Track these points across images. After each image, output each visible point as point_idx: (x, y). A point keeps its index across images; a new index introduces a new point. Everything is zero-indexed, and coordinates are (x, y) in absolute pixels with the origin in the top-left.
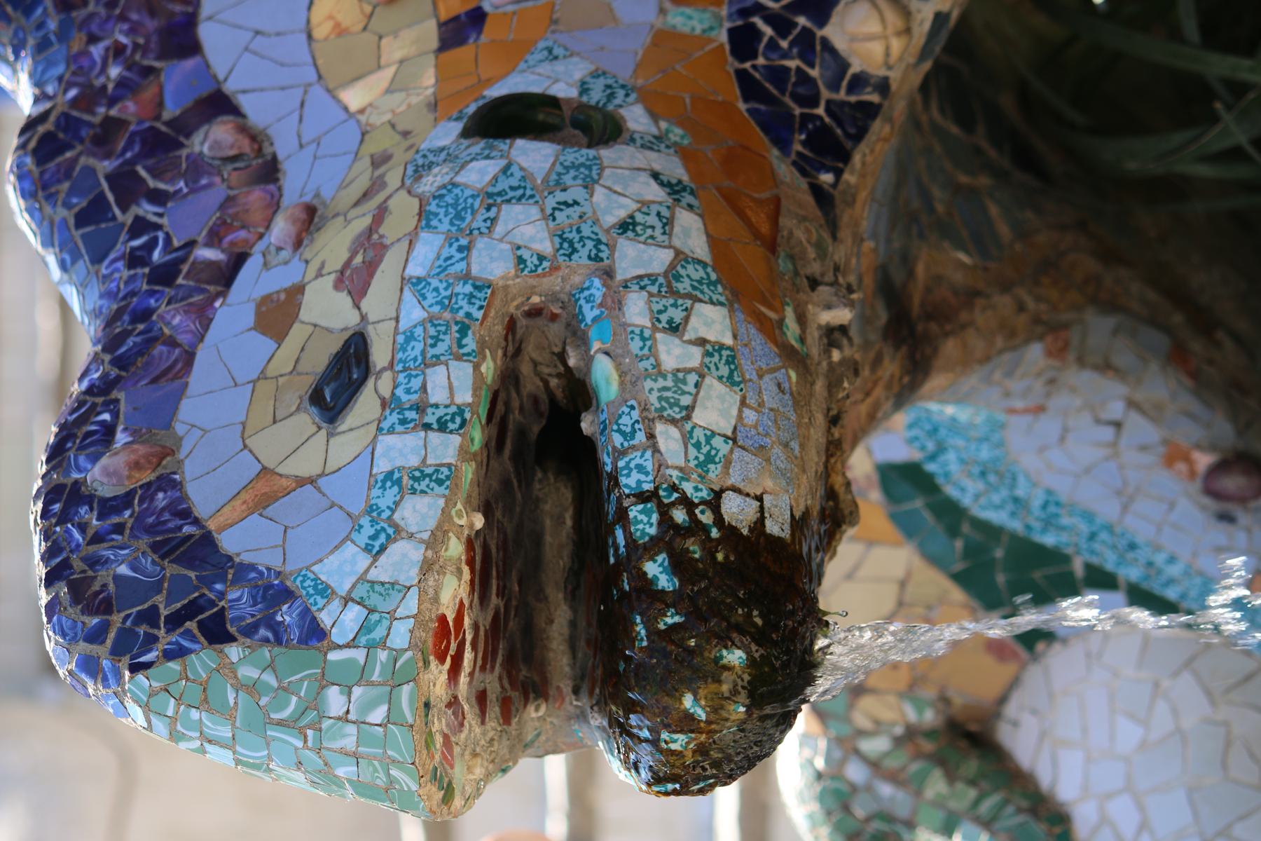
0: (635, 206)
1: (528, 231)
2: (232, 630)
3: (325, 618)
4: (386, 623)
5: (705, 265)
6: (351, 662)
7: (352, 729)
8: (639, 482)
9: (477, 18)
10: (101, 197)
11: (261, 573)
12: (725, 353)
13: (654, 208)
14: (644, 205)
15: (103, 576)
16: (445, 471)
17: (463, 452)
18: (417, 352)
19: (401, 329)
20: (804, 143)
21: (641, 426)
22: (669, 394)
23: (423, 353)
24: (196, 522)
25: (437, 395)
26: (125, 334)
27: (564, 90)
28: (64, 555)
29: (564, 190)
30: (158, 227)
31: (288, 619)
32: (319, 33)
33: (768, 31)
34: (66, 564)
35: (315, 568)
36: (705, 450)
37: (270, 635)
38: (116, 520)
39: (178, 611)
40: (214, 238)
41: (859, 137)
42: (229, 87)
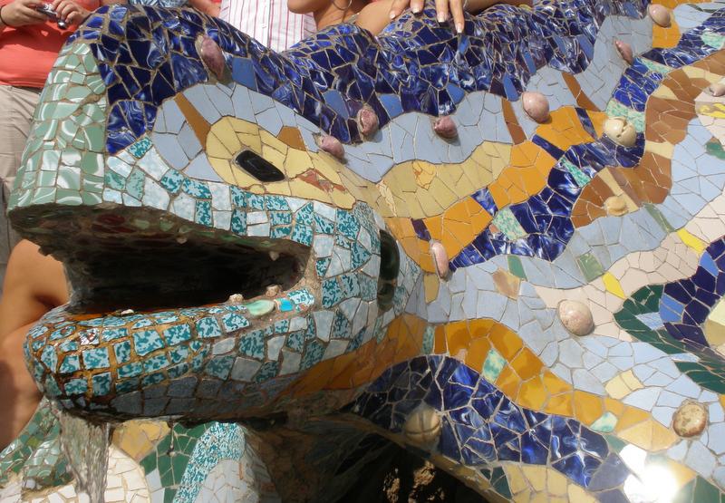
0: (350, 319)
2: (117, 103)
3: (123, 154)
4: (119, 188)
5: (320, 358)
6: (95, 167)
7: (54, 167)
8: (203, 329)
10: (342, 62)
11: (150, 120)
12: (274, 372)
13: (349, 330)
14: (351, 323)
15: (149, 37)
16: (209, 222)
17: (222, 232)
18: (275, 207)
19: (287, 199)
20: (373, 397)
21: (235, 329)
22: (252, 344)
23: (274, 210)
24: (182, 88)
25: (252, 218)
26: (280, 65)
27: (400, 279)
28: (162, 18)
29: (358, 283)
30: (330, 86)
31: (123, 133)
33: (423, 376)
34: (157, 19)
35: (153, 149)
36: (221, 365)
37: (113, 123)
38: (182, 46)
39: (128, 73)
40: (325, 111)
41: (374, 421)
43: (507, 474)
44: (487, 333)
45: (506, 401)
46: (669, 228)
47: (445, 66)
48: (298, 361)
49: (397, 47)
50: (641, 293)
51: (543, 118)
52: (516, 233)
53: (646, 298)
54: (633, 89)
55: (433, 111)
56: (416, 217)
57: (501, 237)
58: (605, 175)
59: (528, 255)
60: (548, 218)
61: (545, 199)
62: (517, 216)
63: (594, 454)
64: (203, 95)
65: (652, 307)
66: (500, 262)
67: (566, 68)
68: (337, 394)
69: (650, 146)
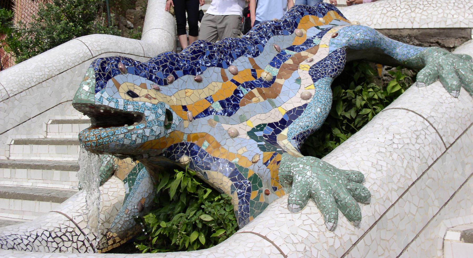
3: (98, 93)
24: (113, 76)
25: (129, 107)
26: (142, 67)
32: (186, 90)
34: (109, 60)
40: (156, 78)
42: (179, 79)
44: (205, 136)
45: (208, 155)
46: (274, 106)
47: (200, 61)
48: (141, 140)
50: (259, 126)
51: (235, 74)
53: (261, 127)
54: (278, 60)
55: (194, 74)
56: (183, 105)
58: (255, 91)
59: (221, 115)
60: (231, 104)
62: (220, 104)
65: (262, 130)
66: (211, 117)
69: (277, 81)
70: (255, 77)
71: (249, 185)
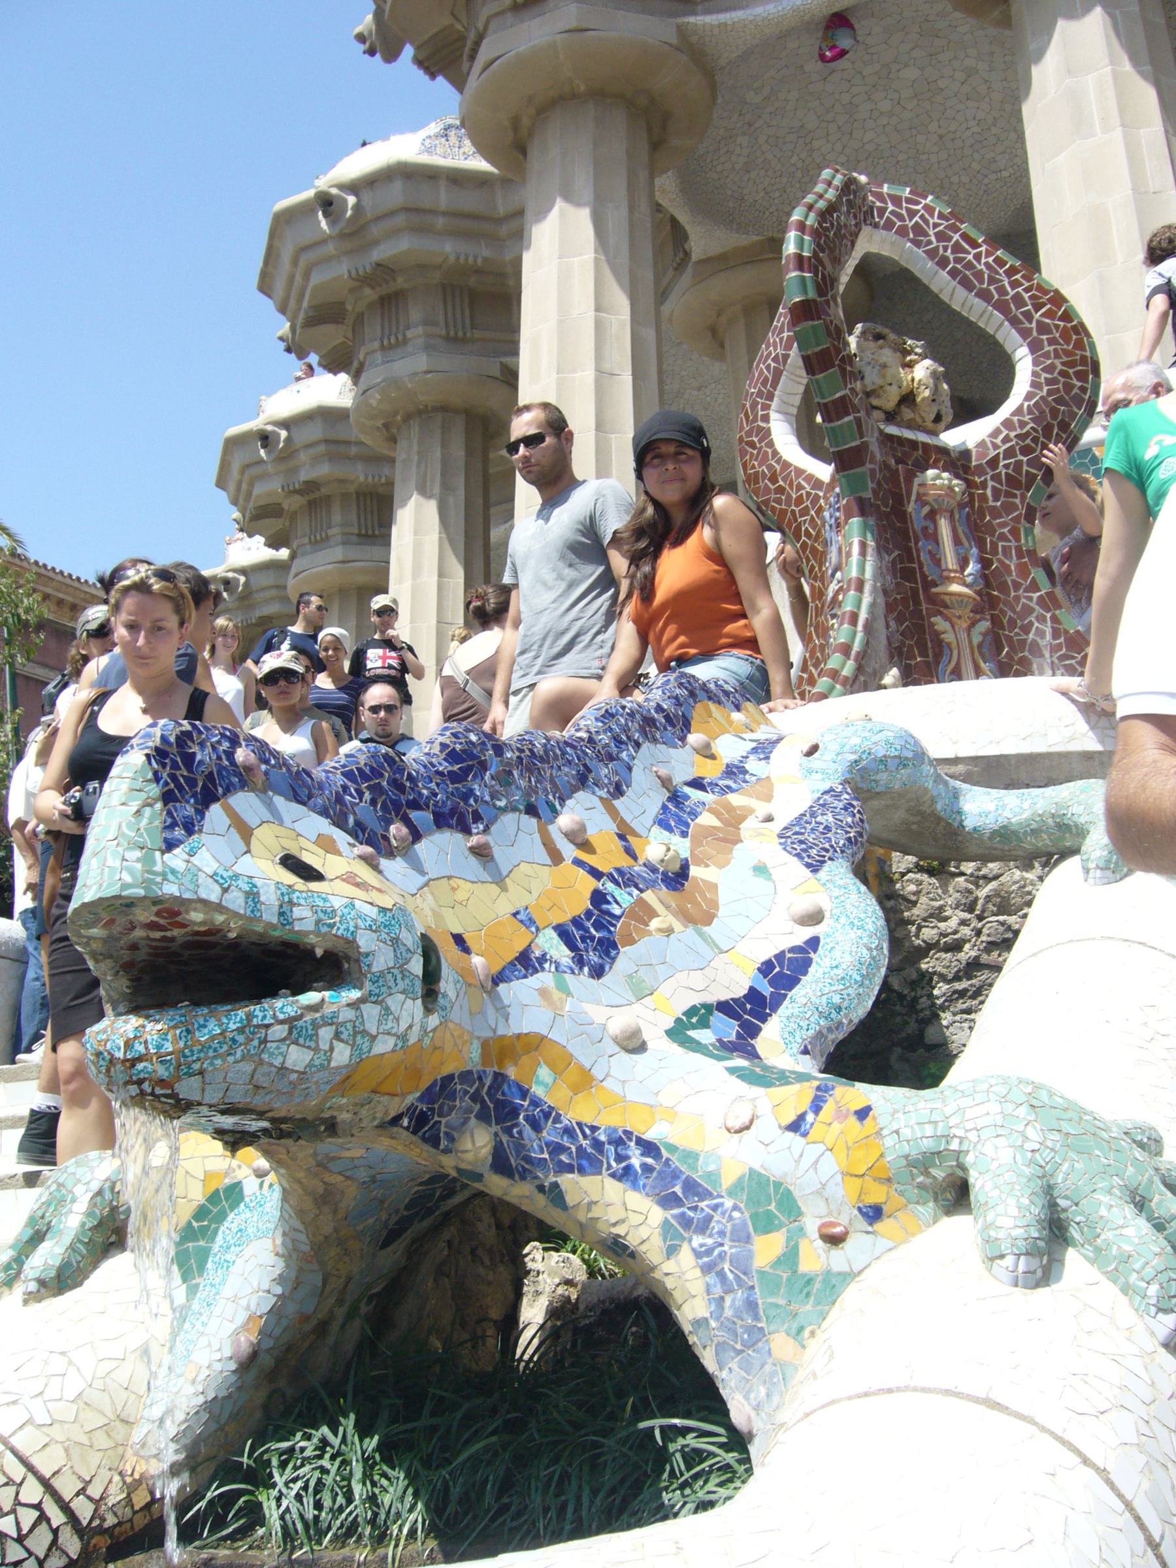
1: (382, 960)
2: (170, 805)
3: (177, 851)
6: (154, 863)
7: (118, 863)
9: (466, 950)
14: (398, 1020)
24: (224, 794)
34: (200, 732)
40: (358, 823)
43: (563, 1188)
45: (558, 1115)
47: (476, 787)
49: (425, 767)
50: (692, 1012)
52: (561, 952)
53: (700, 1015)
56: (455, 931)
57: (544, 955)
58: (649, 896)
60: (592, 938)
61: (589, 919)
63: (650, 1161)
64: (244, 802)
65: (704, 1024)
66: (544, 979)
67: (603, 793)
68: (385, 1099)
69: (694, 871)
70: (635, 858)
71: (736, 1214)
